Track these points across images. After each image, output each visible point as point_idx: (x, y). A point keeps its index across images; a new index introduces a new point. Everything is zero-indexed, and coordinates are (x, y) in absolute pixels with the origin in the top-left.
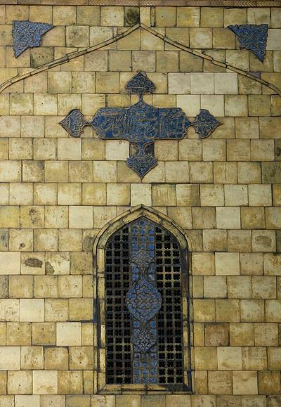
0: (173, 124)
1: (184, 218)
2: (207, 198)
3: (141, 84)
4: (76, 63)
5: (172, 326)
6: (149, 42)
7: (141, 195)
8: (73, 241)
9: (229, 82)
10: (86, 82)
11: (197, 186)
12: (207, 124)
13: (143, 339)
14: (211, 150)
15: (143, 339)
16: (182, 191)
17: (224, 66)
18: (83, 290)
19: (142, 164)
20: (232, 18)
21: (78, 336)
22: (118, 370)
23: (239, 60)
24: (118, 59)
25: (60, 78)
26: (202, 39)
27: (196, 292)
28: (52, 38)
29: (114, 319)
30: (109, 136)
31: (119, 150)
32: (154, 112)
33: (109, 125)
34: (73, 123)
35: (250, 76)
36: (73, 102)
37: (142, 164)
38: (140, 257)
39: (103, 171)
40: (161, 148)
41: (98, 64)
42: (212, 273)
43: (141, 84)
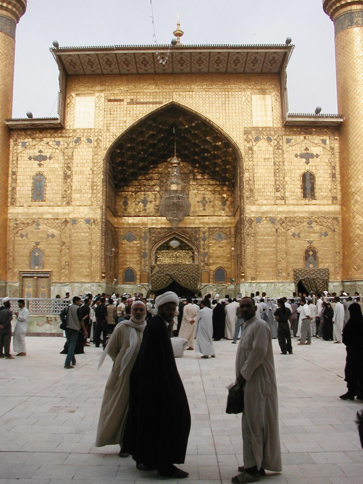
0: (312, 156)
1: (314, 172)
2: (318, 168)
3: (307, 149)
4: (296, 145)
5: (313, 189)
6: (308, 142)
7: (308, 168)
8: (297, 175)
9: (321, 149)
10: (298, 148)
11: (316, 166)
12: (317, 156)
13: (309, 191)
14: (318, 160)
15: (309, 191)
16: (314, 167)
17: (320, 146)
18: (299, 183)
19: (307, 163)
20: (321, 138)
21: (299, 192)
22: (305, 196)
23: (323, 145)
24: (303, 145)
25: (294, 148)
26: (316, 142)
27: (316, 184)
28: (292, 141)
29: (304, 188)
30: (302, 158)
31: (304, 160)
32: (309, 154)
33: (302, 156)
34: (296, 156)
35: (324, 148)
36: (296, 152)
37: (307, 163)
38: (308, 178)
39: (301, 164)
40: (310, 160)
41: (299, 145)
42: (319, 182)
43: (307, 149)
